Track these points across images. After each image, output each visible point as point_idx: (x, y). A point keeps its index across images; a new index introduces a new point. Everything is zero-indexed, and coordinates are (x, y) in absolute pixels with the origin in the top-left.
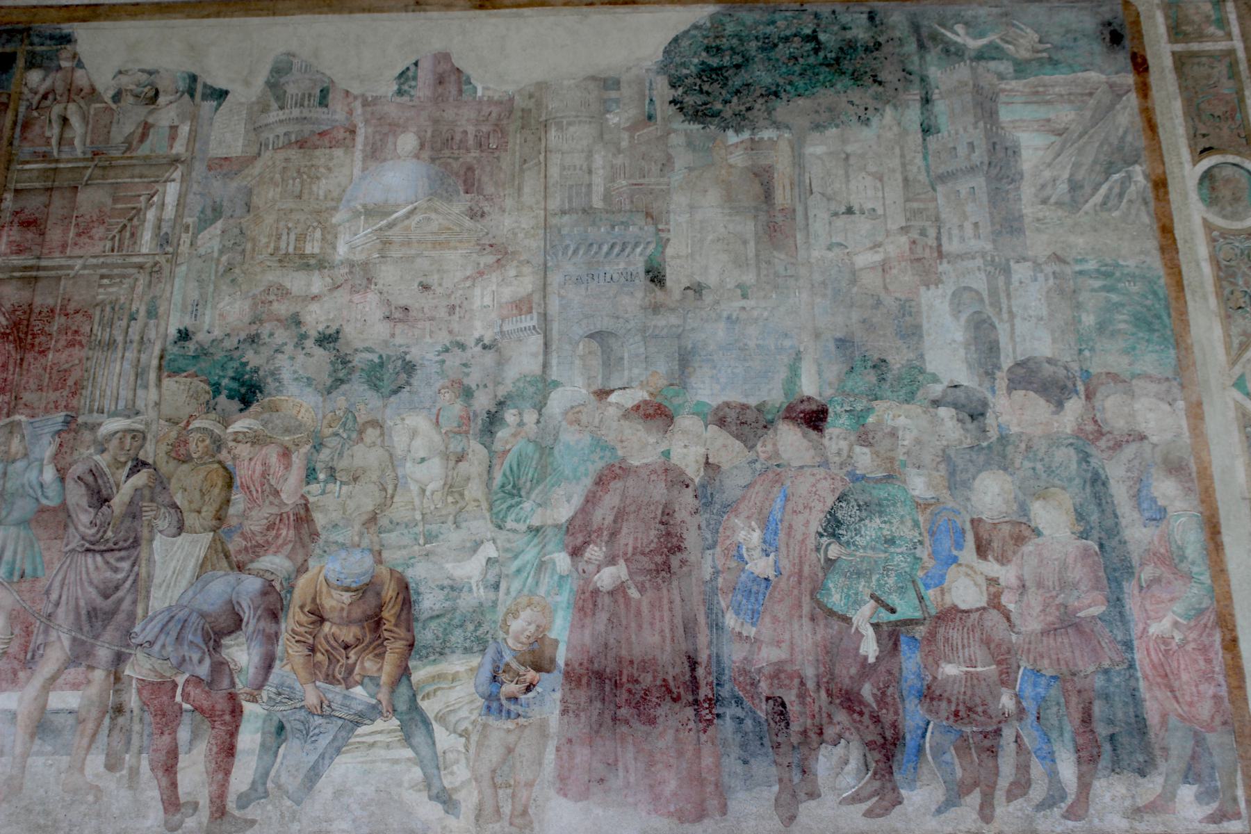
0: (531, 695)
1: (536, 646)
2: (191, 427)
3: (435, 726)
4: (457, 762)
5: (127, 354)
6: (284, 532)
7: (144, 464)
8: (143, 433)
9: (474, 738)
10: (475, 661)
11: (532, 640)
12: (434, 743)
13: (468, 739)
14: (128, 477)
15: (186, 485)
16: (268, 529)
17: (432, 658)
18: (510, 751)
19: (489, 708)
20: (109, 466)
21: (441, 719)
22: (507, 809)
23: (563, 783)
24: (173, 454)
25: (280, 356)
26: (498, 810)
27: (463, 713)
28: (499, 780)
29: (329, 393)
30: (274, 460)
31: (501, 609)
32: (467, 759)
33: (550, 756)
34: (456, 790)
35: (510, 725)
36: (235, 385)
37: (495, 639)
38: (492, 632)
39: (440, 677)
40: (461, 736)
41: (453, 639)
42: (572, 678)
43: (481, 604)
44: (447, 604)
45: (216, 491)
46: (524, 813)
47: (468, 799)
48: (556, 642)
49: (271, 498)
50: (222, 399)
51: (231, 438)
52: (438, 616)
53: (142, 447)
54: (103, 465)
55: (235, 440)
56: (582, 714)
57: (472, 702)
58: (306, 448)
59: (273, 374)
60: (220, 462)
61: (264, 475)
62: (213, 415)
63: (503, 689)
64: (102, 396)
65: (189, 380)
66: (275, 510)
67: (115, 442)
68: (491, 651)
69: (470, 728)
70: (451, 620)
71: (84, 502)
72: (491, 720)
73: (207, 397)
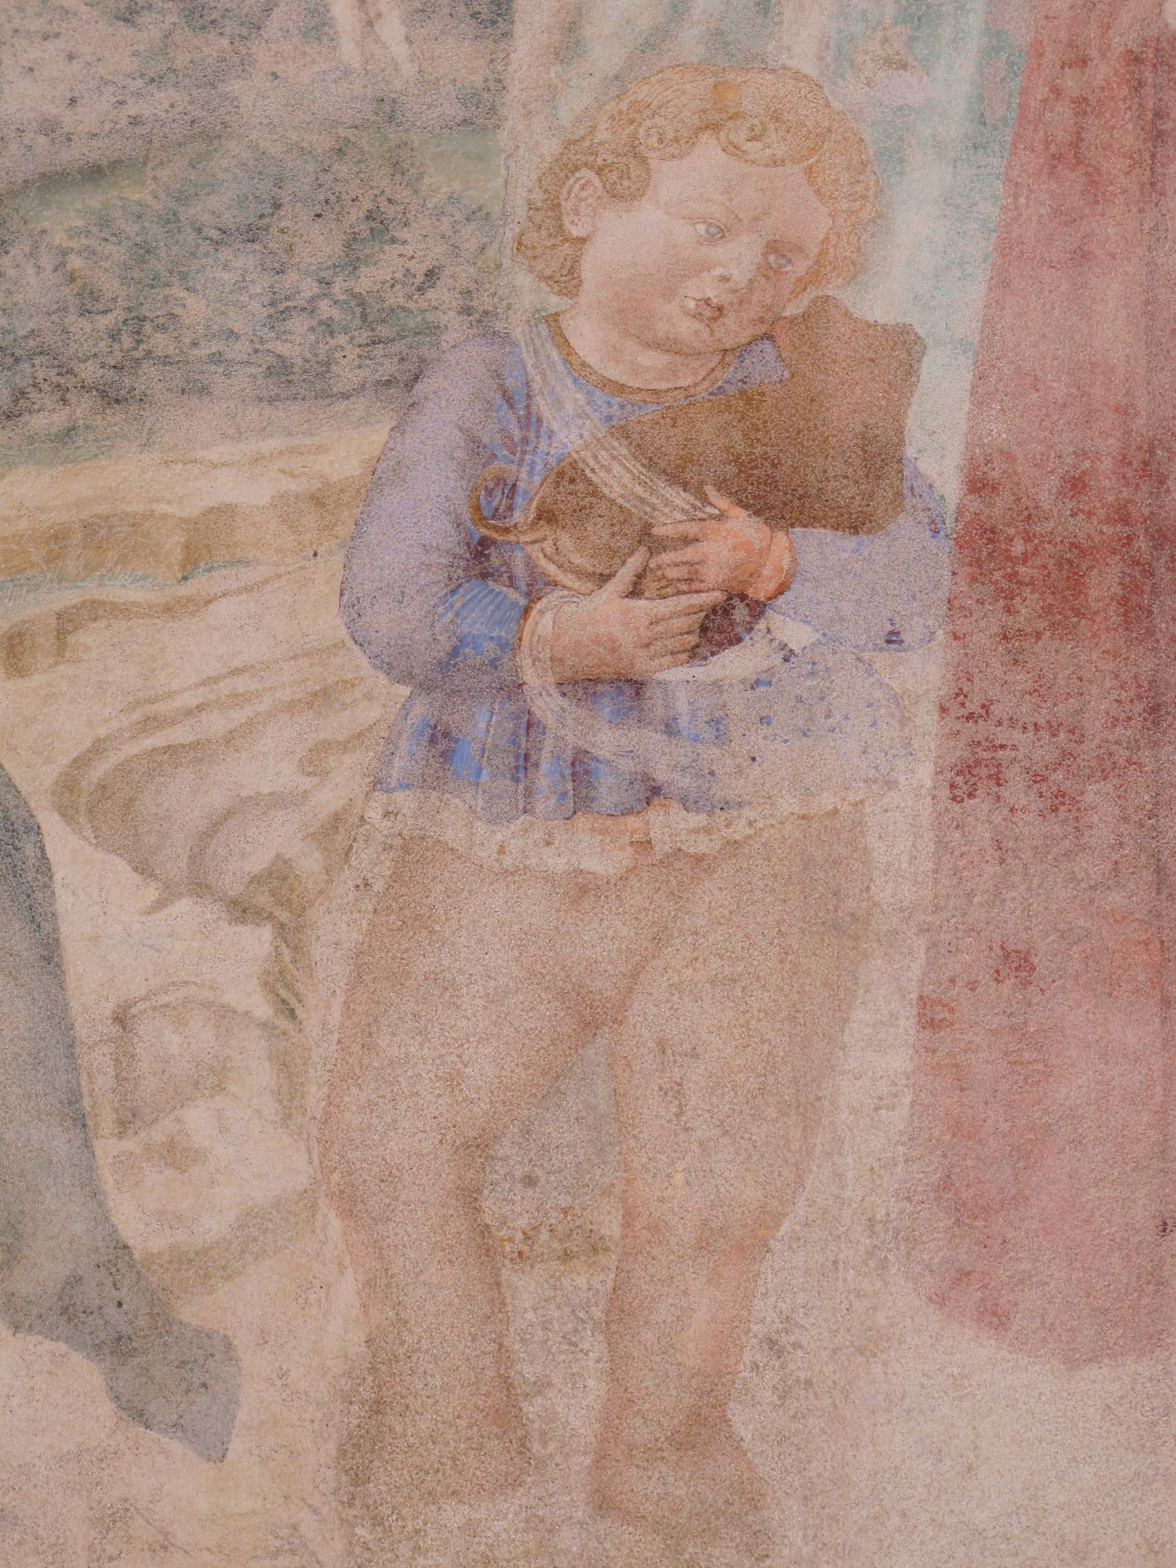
0: (734, 664)
1: (765, 367)
3: (63, 844)
4: (214, 1079)
9: (335, 932)
10: (346, 447)
11: (734, 331)
12: (50, 955)
13: (292, 936)
17: (47, 419)
18: (590, 1016)
19: (441, 740)
21: (107, 801)
22: (572, 1405)
23: (975, 1233)
26: (505, 1412)
27: (266, 767)
28: (510, 1210)
31: (527, 147)
32: (288, 1067)
33: (878, 1059)
34: (202, 1265)
35: (591, 851)
37: (483, 321)
38: (465, 274)
39: (102, 539)
40: (241, 911)
41: (195, 309)
42: (1009, 555)
43: (388, 110)
44: (157, 104)
46: (701, 1429)
47: (290, 1334)
48: (901, 350)
52: (94, 173)
56: (1093, 793)
57: (322, 698)
63: (543, 622)
68: (452, 397)
69: (310, 863)
70: (183, 198)
72: (459, 820)
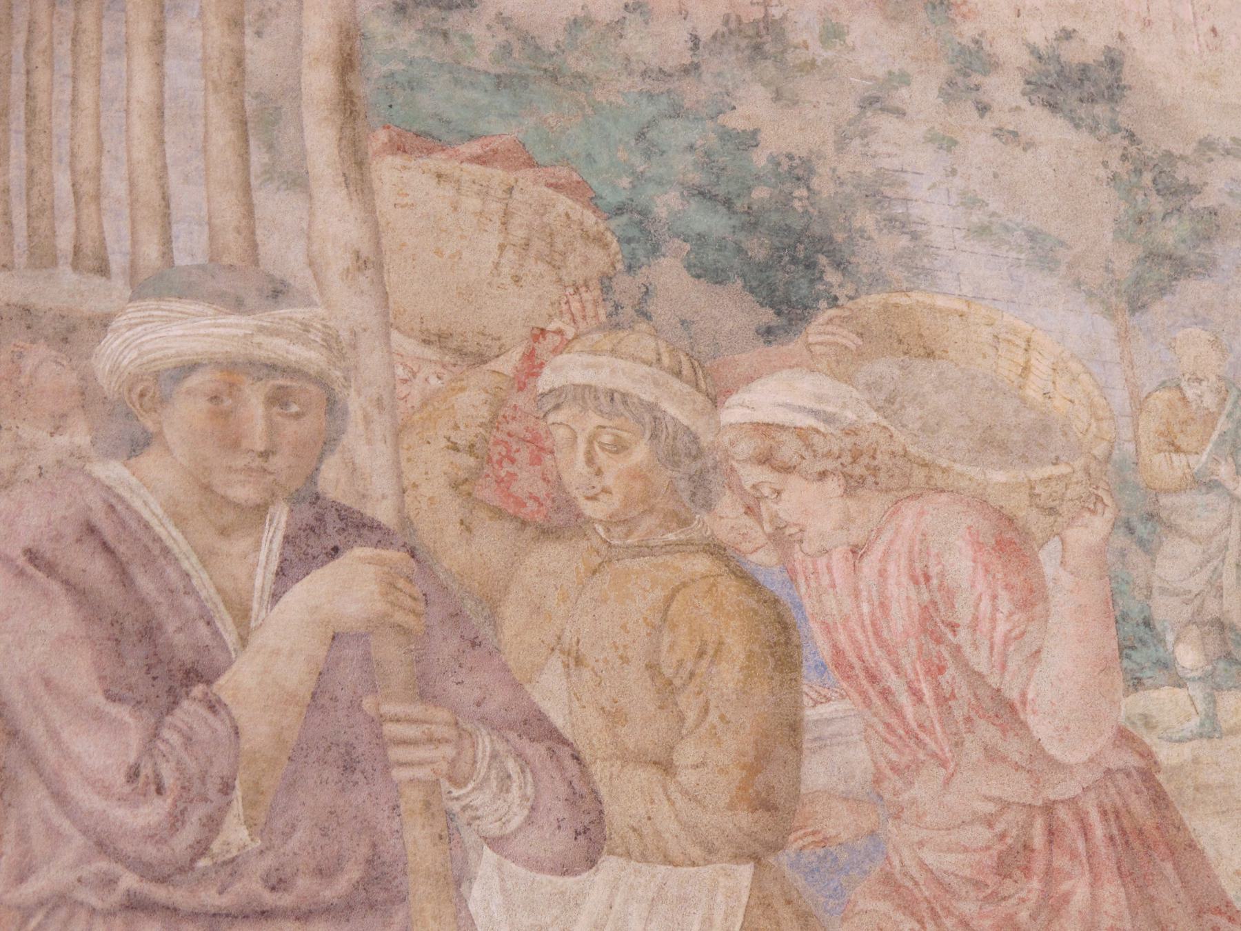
2: (547, 380)
5: (175, 29)
6: (1080, 892)
7: (358, 526)
8: (321, 381)
14: (285, 575)
15: (575, 627)
16: (1003, 868)
20: (180, 520)
24: (487, 493)
25: (888, 125)
29: (1136, 306)
30: (960, 563)
36: (713, 222)
45: (727, 676)
49: (987, 731)
50: (669, 272)
51: (745, 448)
53: (328, 443)
54: (150, 508)
55: (765, 459)
58: (1091, 531)
59: (875, 195)
60: (716, 550)
61: (934, 623)
62: (641, 341)
64: (88, 193)
65: (497, 175)
66: (1017, 788)
67: (185, 415)
71: (80, 672)
73: (599, 259)
